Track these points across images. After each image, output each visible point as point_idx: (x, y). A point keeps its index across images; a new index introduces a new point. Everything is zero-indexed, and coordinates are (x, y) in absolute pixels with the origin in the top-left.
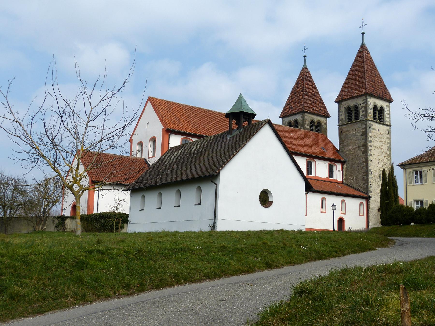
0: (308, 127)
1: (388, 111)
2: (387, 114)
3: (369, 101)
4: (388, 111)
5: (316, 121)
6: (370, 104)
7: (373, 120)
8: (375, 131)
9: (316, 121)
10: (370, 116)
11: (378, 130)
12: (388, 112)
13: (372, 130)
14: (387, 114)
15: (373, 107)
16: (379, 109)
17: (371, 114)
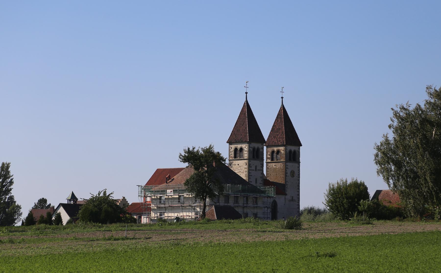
0: (269, 157)
1: (246, 149)
2: (245, 151)
3: (230, 147)
4: (246, 149)
5: (276, 150)
6: (232, 148)
7: (234, 159)
8: (235, 166)
9: (276, 150)
10: (231, 157)
11: (238, 165)
12: (247, 150)
13: (233, 166)
14: (245, 151)
15: (234, 150)
16: (239, 150)
17: (232, 156)
